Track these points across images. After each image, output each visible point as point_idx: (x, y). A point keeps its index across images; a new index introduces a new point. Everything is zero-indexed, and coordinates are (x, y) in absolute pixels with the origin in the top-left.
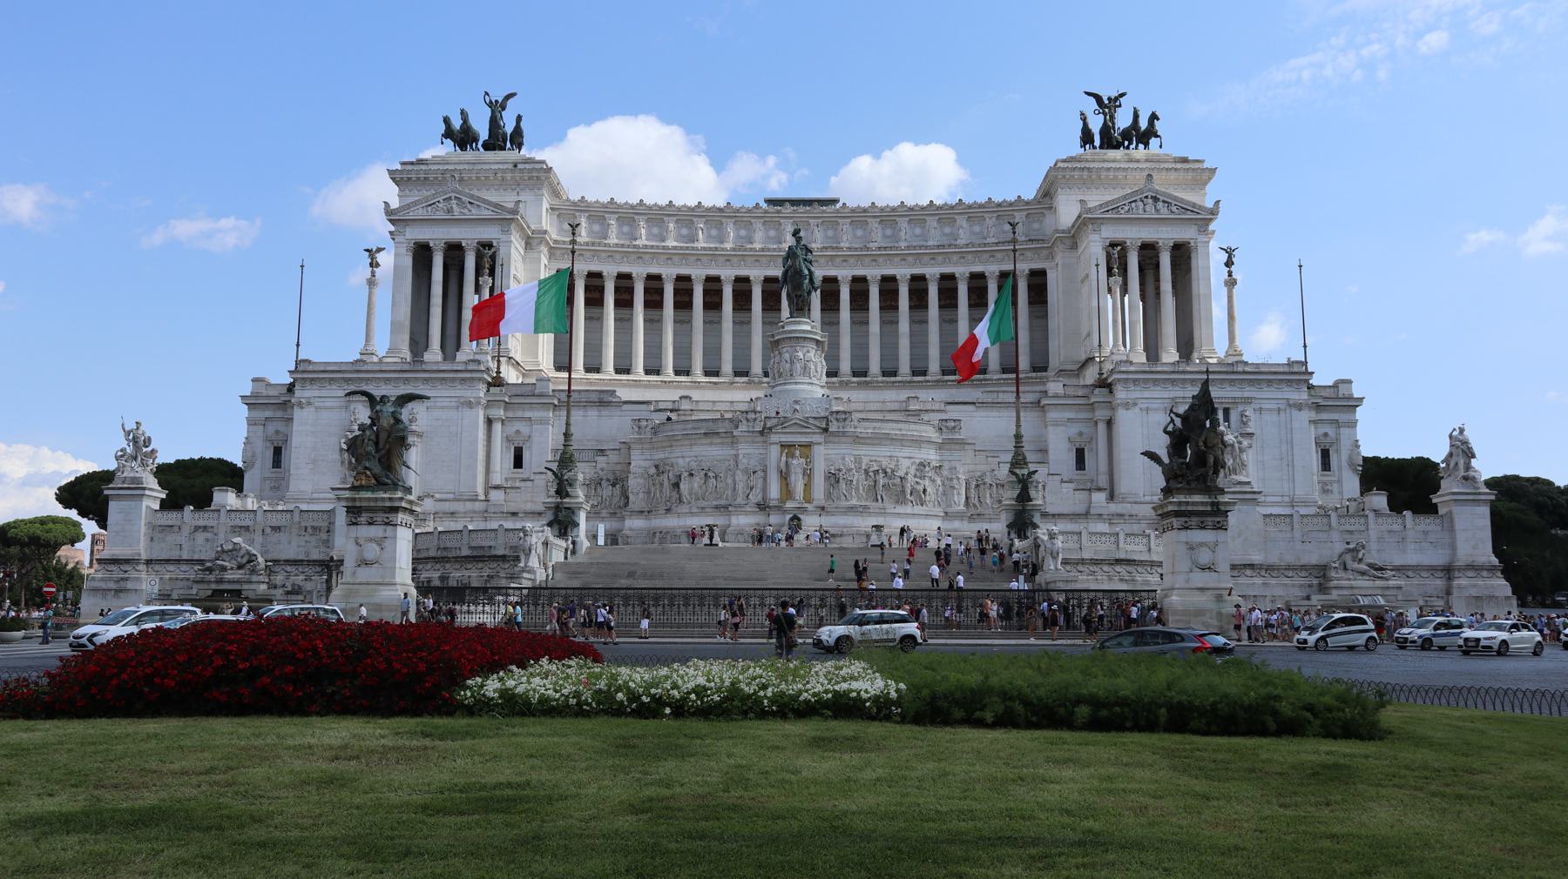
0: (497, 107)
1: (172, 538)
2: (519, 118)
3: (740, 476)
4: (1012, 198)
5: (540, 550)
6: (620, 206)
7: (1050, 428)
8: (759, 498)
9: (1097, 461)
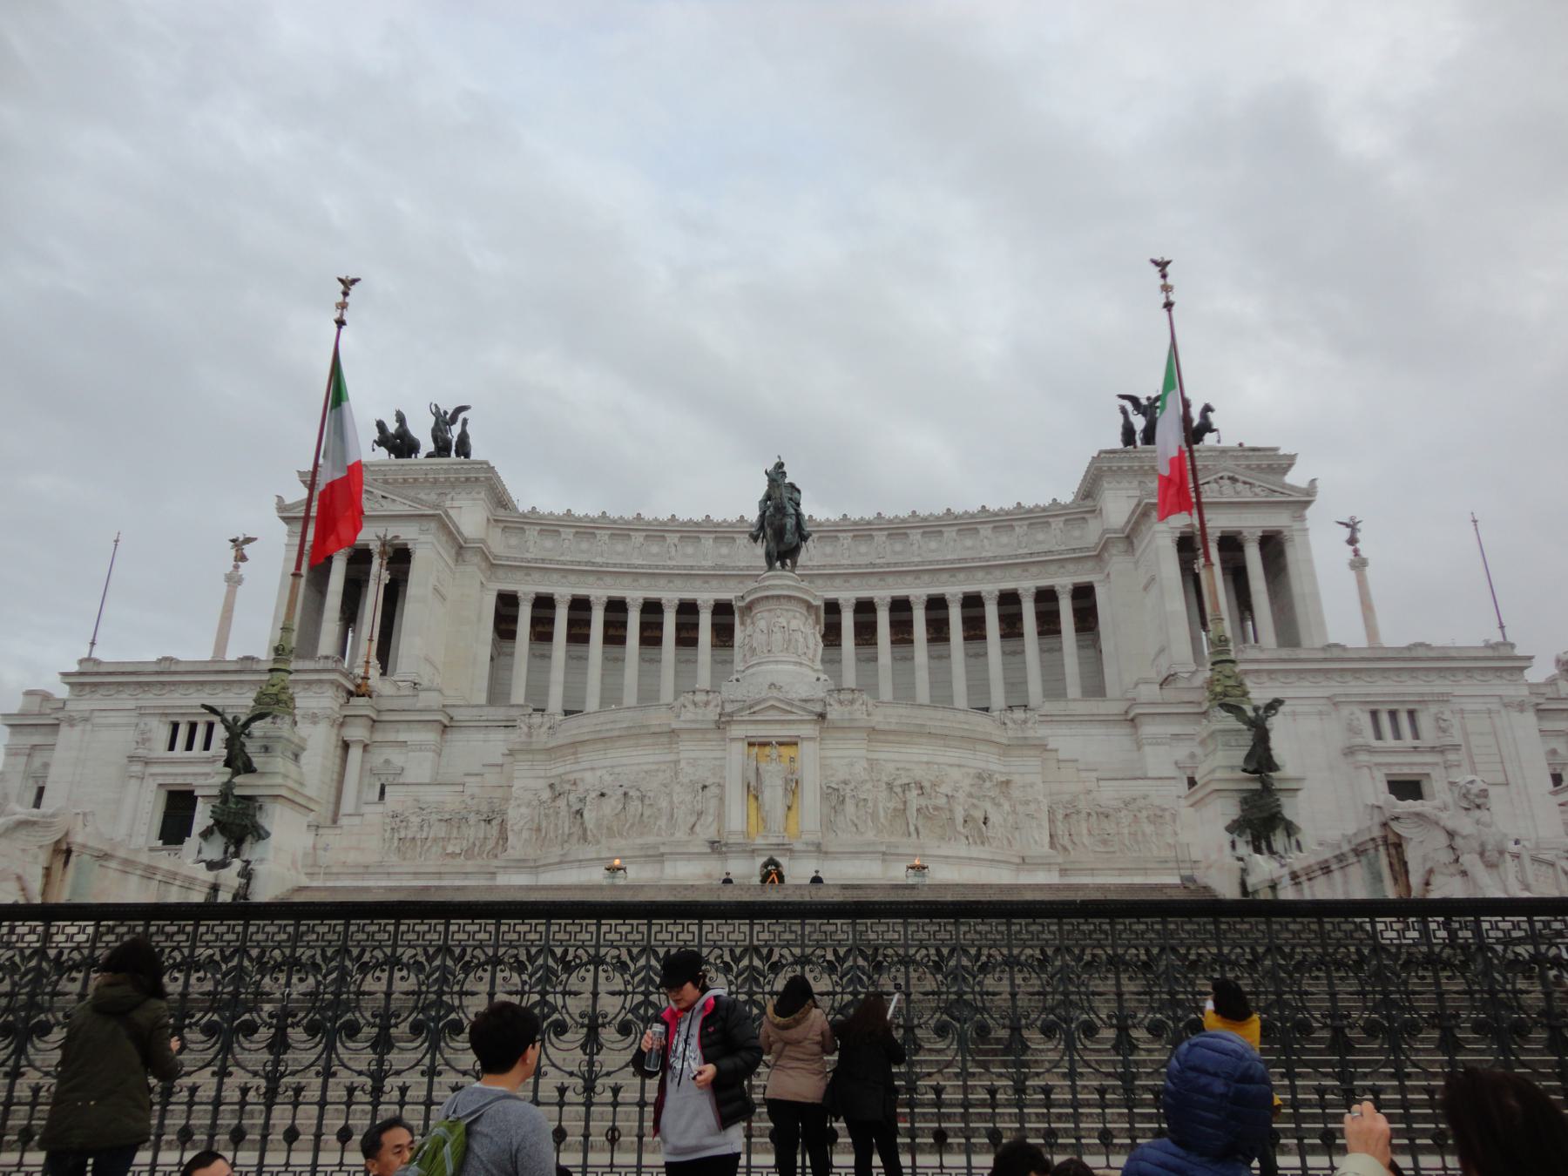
2: (465, 422)
6: (579, 519)
7: (1147, 749)
8: (712, 833)
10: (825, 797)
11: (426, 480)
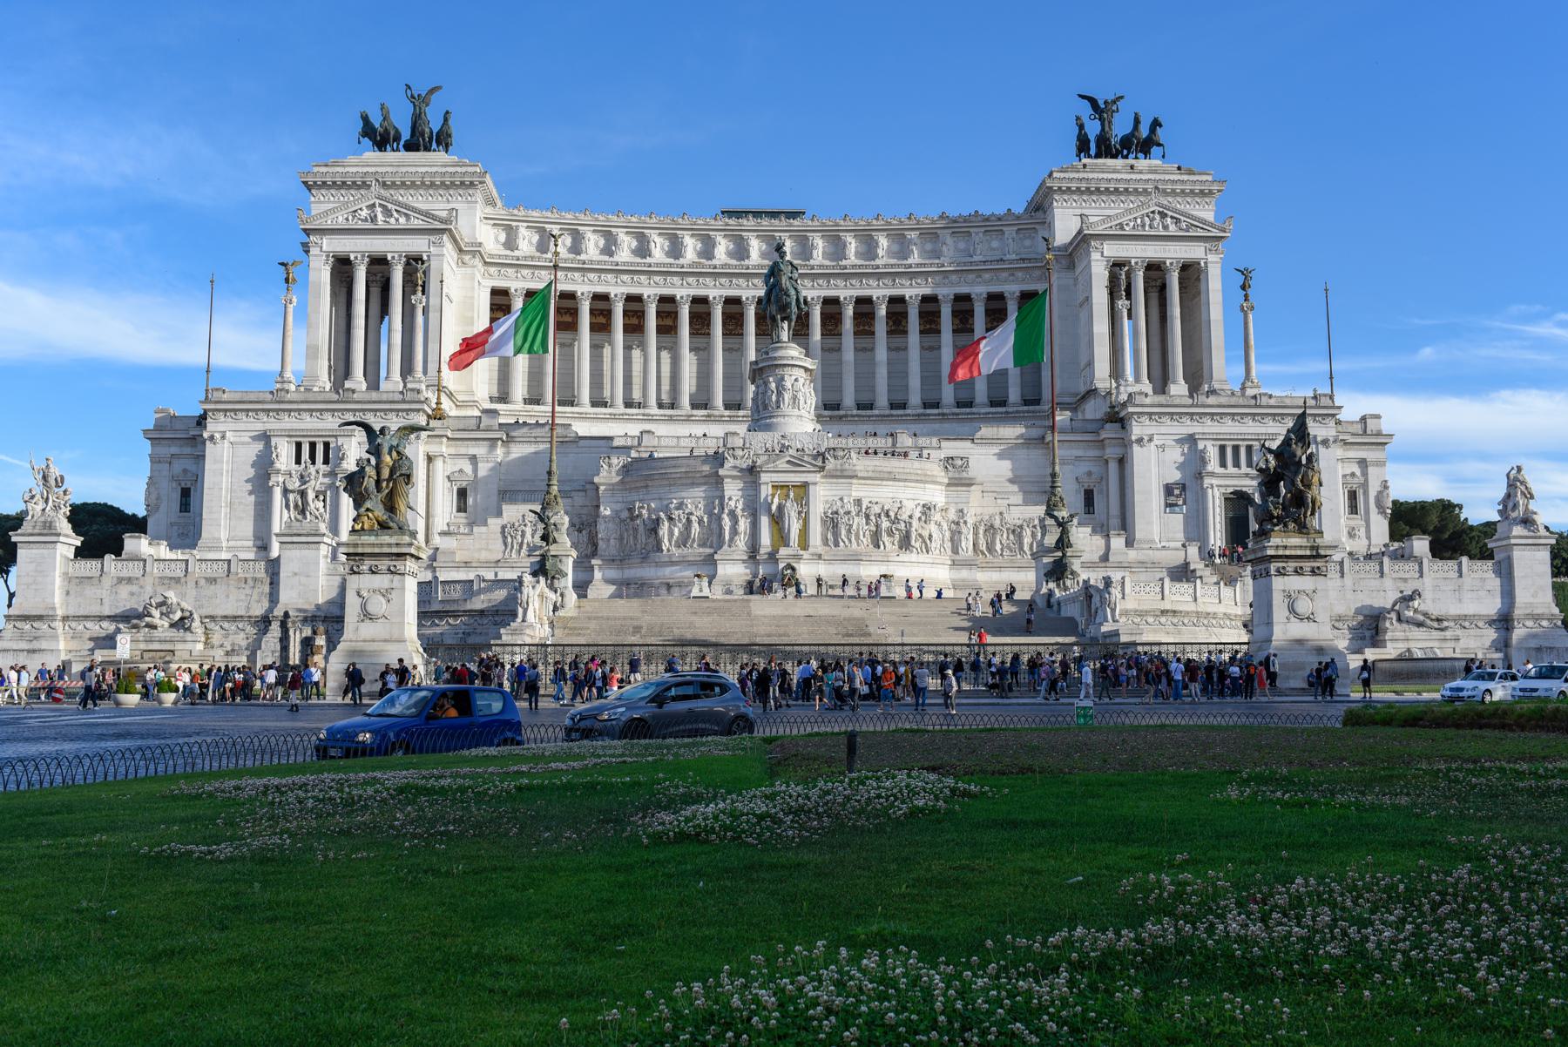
0: (419, 102)
1: (91, 591)
3: (727, 522)
4: (1000, 211)
5: (537, 605)
9: (1108, 503)
10: (824, 522)
11: (423, 183)
